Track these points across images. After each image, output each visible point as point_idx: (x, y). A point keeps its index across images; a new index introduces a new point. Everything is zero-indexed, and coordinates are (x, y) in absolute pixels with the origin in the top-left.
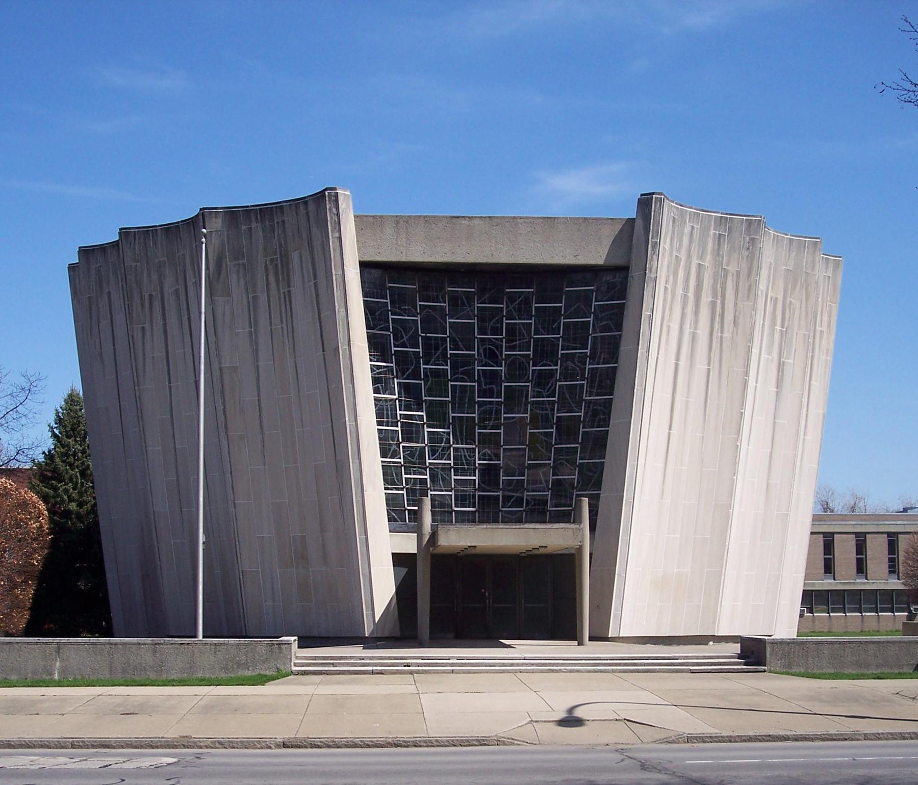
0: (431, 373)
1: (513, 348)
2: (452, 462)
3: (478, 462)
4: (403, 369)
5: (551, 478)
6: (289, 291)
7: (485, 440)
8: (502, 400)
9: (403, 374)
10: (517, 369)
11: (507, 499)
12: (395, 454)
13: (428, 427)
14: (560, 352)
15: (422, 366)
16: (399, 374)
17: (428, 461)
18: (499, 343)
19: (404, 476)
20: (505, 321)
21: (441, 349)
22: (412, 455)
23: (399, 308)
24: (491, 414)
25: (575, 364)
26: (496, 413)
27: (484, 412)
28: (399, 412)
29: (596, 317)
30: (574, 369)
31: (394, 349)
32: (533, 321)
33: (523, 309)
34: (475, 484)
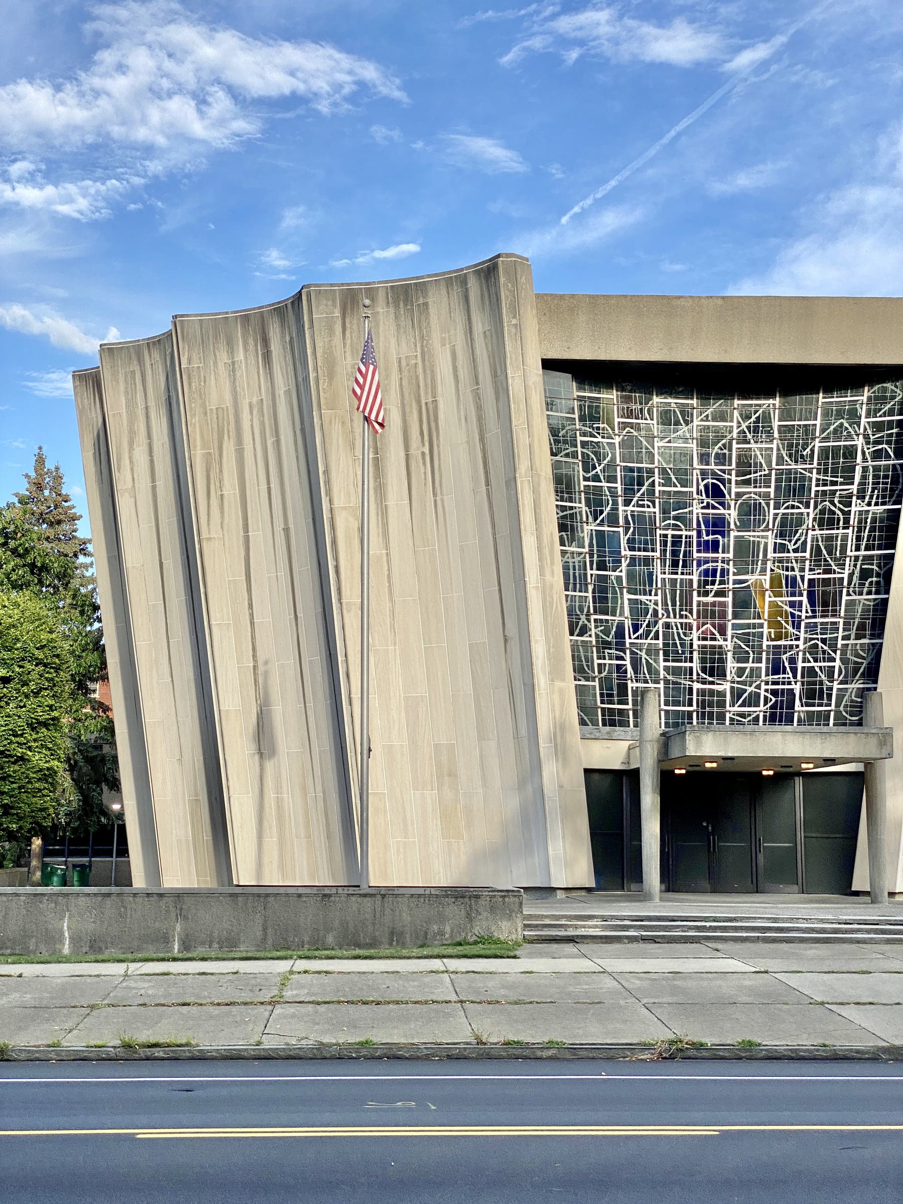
0: (633, 516)
1: (747, 482)
2: (660, 642)
4: (595, 511)
5: (800, 665)
6: (435, 402)
7: (706, 613)
8: (731, 555)
9: (595, 519)
10: (751, 514)
11: (737, 694)
12: (584, 631)
14: (814, 489)
15: (621, 508)
16: (591, 519)
17: (628, 641)
18: (726, 476)
19: (596, 662)
20: (735, 446)
21: (646, 484)
22: (607, 632)
23: (591, 427)
24: (714, 575)
25: (835, 506)
26: (722, 575)
27: (706, 572)
28: (589, 572)
29: (866, 437)
30: (834, 513)
31: (583, 483)
32: (774, 446)
33: (761, 427)
34: (691, 674)
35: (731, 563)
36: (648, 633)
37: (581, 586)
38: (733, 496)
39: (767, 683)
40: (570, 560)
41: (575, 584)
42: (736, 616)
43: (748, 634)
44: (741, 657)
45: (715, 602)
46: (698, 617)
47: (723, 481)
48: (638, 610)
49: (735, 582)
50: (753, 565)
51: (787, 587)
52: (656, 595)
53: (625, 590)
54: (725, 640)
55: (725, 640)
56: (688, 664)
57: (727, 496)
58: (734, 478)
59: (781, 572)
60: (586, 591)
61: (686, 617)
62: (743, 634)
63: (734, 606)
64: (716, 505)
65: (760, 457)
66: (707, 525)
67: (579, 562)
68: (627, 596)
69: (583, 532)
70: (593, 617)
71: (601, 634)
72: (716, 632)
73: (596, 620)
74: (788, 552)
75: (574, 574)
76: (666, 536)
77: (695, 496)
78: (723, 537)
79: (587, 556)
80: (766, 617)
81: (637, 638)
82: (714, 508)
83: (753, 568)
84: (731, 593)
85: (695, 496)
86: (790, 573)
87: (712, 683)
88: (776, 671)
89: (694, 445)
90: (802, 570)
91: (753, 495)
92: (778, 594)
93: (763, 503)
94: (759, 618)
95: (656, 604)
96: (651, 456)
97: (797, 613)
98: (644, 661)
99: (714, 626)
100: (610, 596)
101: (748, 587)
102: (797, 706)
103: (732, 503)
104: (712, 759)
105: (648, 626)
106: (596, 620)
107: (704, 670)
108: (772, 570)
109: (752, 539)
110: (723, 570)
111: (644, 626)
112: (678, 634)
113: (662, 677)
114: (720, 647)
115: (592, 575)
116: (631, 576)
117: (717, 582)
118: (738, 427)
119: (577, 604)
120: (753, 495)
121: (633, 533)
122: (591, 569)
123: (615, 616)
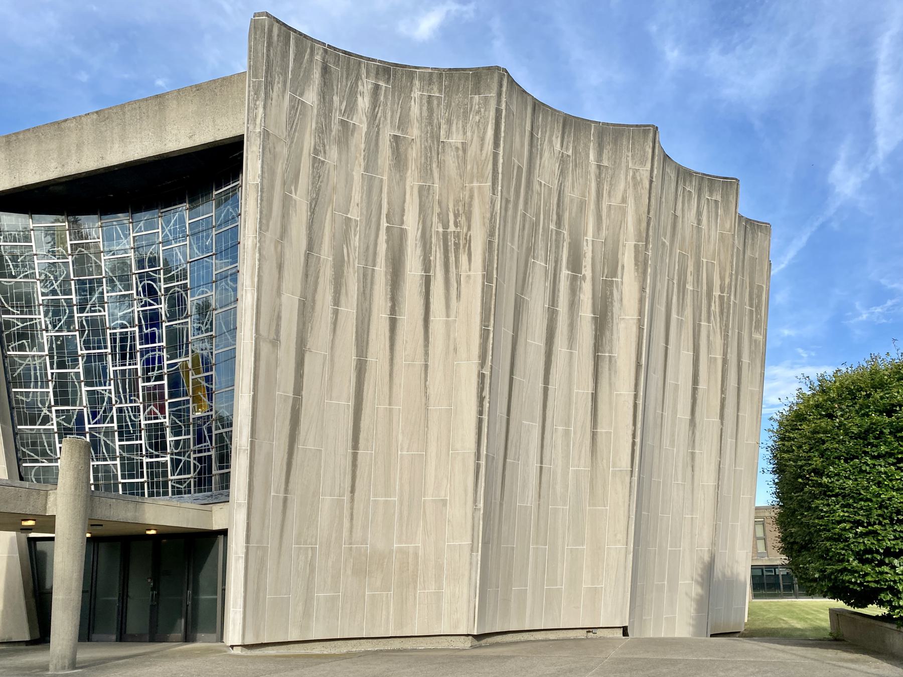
0: (87, 321)
2: (115, 425)
3: (143, 422)
5: (214, 432)
13: (87, 385)
24: (154, 363)
26: (160, 362)
27: (147, 360)
28: (49, 371)
31: (41, 298)
36: (105, 418)
37: (42, 382)
38: (163, 292)
39: (195, 452)
40: (31, 363)
41: (36, 382)
42: (170, 397)
43: (179, 410)
44: (176, 431)
46: (144, 400)
47: (154, 280)
48: (95, 399)
49: (169, 366)
52: (110, 385)
53: (83, 384)
54: (165, 418)
55: (165, 418)
56: (139, 442)
57: (159, 293)
58: (162, 277)
60: (48, 387)
61: (135, 401)
63: (169, 388)
66: (146, 321)
67: (40, 363)
68: (84, 389)
69: (43, 339)
70: (54, 409)
71: (63, 422)
72: (157, 412)
73: (57, 411)
75: (35, 374)
76: (115, 334)
77: (135, 296)
78: (158, 329)
79: (47, 358)
81: (96, 423)
82: (150, 305)
84: (166, 377)
85: (135, 296)
87: (157, 456)
88: (200, 442)
89: (131, 254)
91: (176, 289)
92: (198, 372)
93: (184, 295)
94: (187, 395)
95: (110, 393)
96: (99, 267)
97: (210, 386)
98: (102, 443)
99: (155, 406)
100: (70, 389)
101: (178, 369)
102: (214, 472)
103: (163, 298)
104: (155, 527)
105: (105, 412)
106: (57, 411)
107: (151, 446)
108: (193, 352)
109: (178, 326)
110: (160, 357)
111: (101, 413)
112: (130, 417)
113: (118, 454)
114: (162, 423)
115: (52, 374)
116: (88, 371)
119: (39, 399)
120: (176, 289)
121: (88, 335)
122: (52, 368)
123: (76, 405)
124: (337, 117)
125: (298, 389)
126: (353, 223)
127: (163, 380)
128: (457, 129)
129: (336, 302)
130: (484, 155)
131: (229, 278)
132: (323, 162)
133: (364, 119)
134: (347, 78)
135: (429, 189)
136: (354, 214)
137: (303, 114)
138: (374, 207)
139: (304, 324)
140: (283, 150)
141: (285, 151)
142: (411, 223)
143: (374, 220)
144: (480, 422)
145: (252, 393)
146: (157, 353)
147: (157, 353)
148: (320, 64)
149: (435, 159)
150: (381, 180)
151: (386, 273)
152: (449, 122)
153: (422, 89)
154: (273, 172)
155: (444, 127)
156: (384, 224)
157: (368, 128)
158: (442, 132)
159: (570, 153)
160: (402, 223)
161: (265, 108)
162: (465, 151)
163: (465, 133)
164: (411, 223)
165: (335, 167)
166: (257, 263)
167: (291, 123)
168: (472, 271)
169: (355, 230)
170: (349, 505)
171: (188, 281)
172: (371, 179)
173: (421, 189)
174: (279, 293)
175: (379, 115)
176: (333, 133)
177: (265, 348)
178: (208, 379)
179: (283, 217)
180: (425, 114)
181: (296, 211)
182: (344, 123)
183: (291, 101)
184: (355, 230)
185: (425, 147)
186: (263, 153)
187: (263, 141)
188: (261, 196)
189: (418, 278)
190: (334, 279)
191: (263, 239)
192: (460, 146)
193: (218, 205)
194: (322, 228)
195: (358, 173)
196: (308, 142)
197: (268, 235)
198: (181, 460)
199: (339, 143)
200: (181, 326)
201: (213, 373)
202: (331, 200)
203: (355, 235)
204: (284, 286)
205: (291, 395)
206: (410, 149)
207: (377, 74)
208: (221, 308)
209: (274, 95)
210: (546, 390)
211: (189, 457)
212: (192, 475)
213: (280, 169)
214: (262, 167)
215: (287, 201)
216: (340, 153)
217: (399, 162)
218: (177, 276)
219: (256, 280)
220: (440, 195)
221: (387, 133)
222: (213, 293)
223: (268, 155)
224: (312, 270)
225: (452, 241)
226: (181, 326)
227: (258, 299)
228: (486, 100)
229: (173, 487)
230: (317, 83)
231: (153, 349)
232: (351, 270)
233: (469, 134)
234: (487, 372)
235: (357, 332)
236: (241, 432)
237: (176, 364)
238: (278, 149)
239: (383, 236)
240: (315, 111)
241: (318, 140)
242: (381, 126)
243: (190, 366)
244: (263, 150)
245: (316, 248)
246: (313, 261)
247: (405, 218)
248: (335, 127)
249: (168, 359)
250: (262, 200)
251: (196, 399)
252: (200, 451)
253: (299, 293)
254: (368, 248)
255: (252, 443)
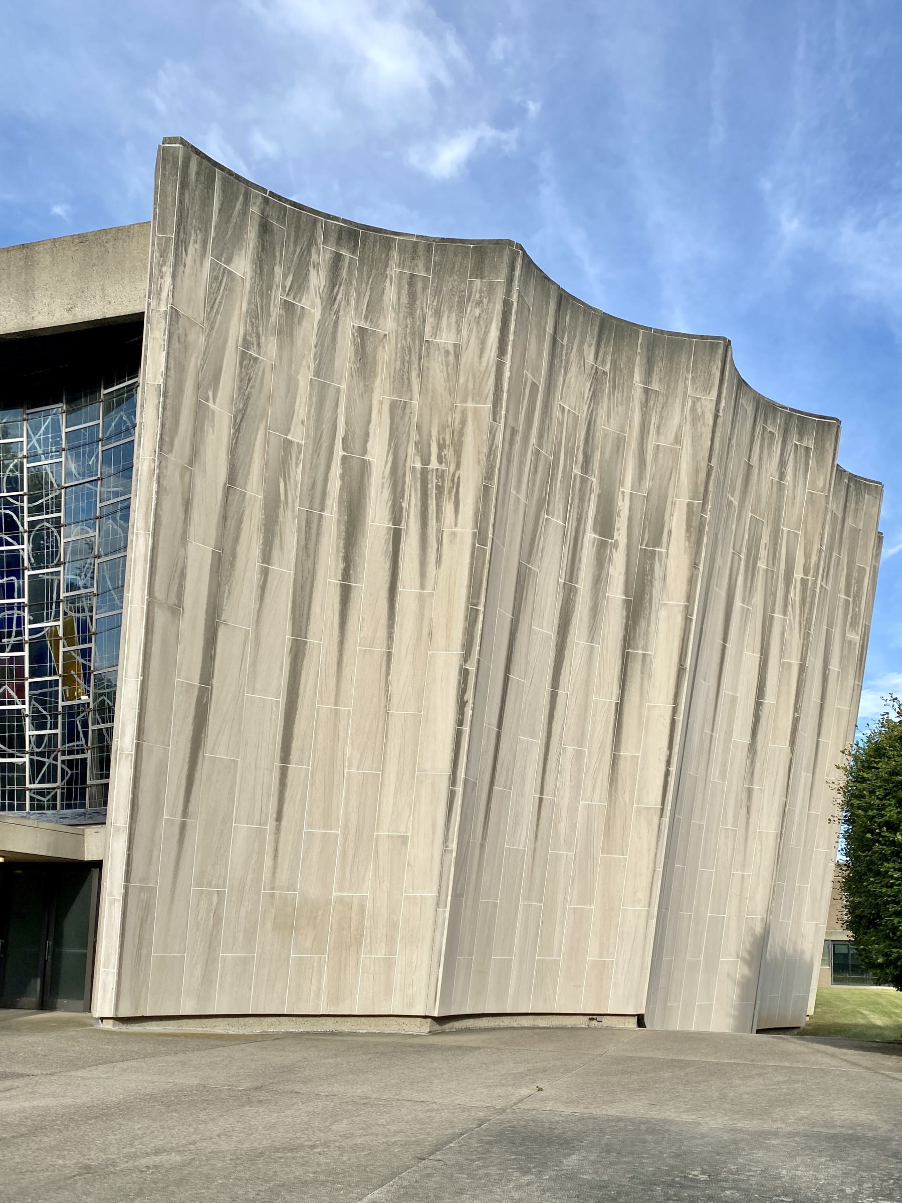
1: (39, 510)
8: (25, 600)
24: (10, 626)
35: (26, 609)
38: (26, 527)
45: (12, 657)
49: (32, 632)
50: (47, 609)
51: (78, 633)
57: (21, 528)
59: (73, 614)
62: (40, 694)
64: (10, 540)
65: (50, 475)
74: (79, 588)
78: (18, 579)
80: (61, 672)
83: (47, 613)
84: (27, 646)
86: (80, 615)
90: (91, 610)
91: (45, 524)
103: (26, 535)
108: (65, 614)
109: (46, 577)
110: (19, 619)
117: (14, 634)
118: (28, 443)
124: (278, 296)
125: (207, 675)
126: (295, 448)
127: (22, 650)
128: (449, 324)
129: (266, 557)
130: (484, 364)
131: (119, 514)
132: (256, 359)
133: (318, 301)
134: (296, 242)
135: (404, 408)
136: (297, 435)
137: (230, 290)
138: (326, 428)
139: (219, 586)
140: (197, 339)
141: (202, 340)
142: (378, 454)
143: (325, 445)
144: (458, 734)
145: (140, 678)
146: (16, 612)
147: (16, 612)
148: (257, 220)
149: (416, 365)
150: (338, 390)
151: (339, 521)
152: (438, 314)
153: (402, 264)
154: (182, 370)
155: (430, 320)
156: (339, 452)
157: (323, 315)
158: (428, 328)
159: (607, 368)
160: (365, 451)
161: (174, 276)
162: (457, 356)
163: (459, 331)
164: (378, 454)
165: (273, 367)
166: (154, 496)
167: (211, 302)
168: (459, 527)
169: (297, 458)
170: (272, 837)
171: (62, 514)
172: (323, 388)
173: (393, 406)
174: (184, 540)
175: (339, 297)
176: (273, 319)
177: (161, 617)
178: (86, 654)
179: (195, 434)
180: (404, 300)
181: (213, 427)
182: (288, 307)
183: (213, 269)
184: (297, 458)
185: (403, 348)
186: (169, 342)
187: (170, 325)
188: (164, 402)
189: (384, 532)
190: (265, 525)
191: (163, 464)
192: (451, 349)
193: (107, 411)
194: (250, 452)
195: (305, 377)
196: (236, 329)
197: (172, 458)
198: (44, 763)
199: (280, 333)
200: (50, 577)
201: (92, 645)
202: (264, 414)
203: (297, 465)
204: (192, 530)
205: (196, 683)
206: (380, 348)
207: (339, 238)
208: (106, 555)
209: (189, 260)
210: (554, 696)
211: (56, 759)
212: (59, 784)
213: (193, 364)
214: (167, 362)
215: (201, 413)
216: (280, 348)
217: (364, 365)
218: (47, 505)
219: (152, 520)
220: (420, 415)
221: (350, 322)
222: (97, 534)
223: (176, 345)
224: (233, 509)
225: (433, 482)
226: (50, 577)
227: (154, 548)
228: (491, 286)
229: (31, 797)
230: (251, 245)
231: (11, 607)
232: (289, 514)
233: (465, 333)
234: (472, 669)
235: (294, 602)
236: (123, 732)
237: (42, 629)
238: (192, 337)
239: (336, 469)
240: (248, 285)
241: (249, 328)
242: (341, 313)
243: (61, 634)
244: (170, 338)
245: (240, 480)
246: (234, 498)
247: (369, 445)
248: (276, 311)
249: (30, 622)
250: (164, 408)
251: (68, 680)
252: (71, 752)
253: (213, 542)
254: (314, 483)
255: (138, 747)
